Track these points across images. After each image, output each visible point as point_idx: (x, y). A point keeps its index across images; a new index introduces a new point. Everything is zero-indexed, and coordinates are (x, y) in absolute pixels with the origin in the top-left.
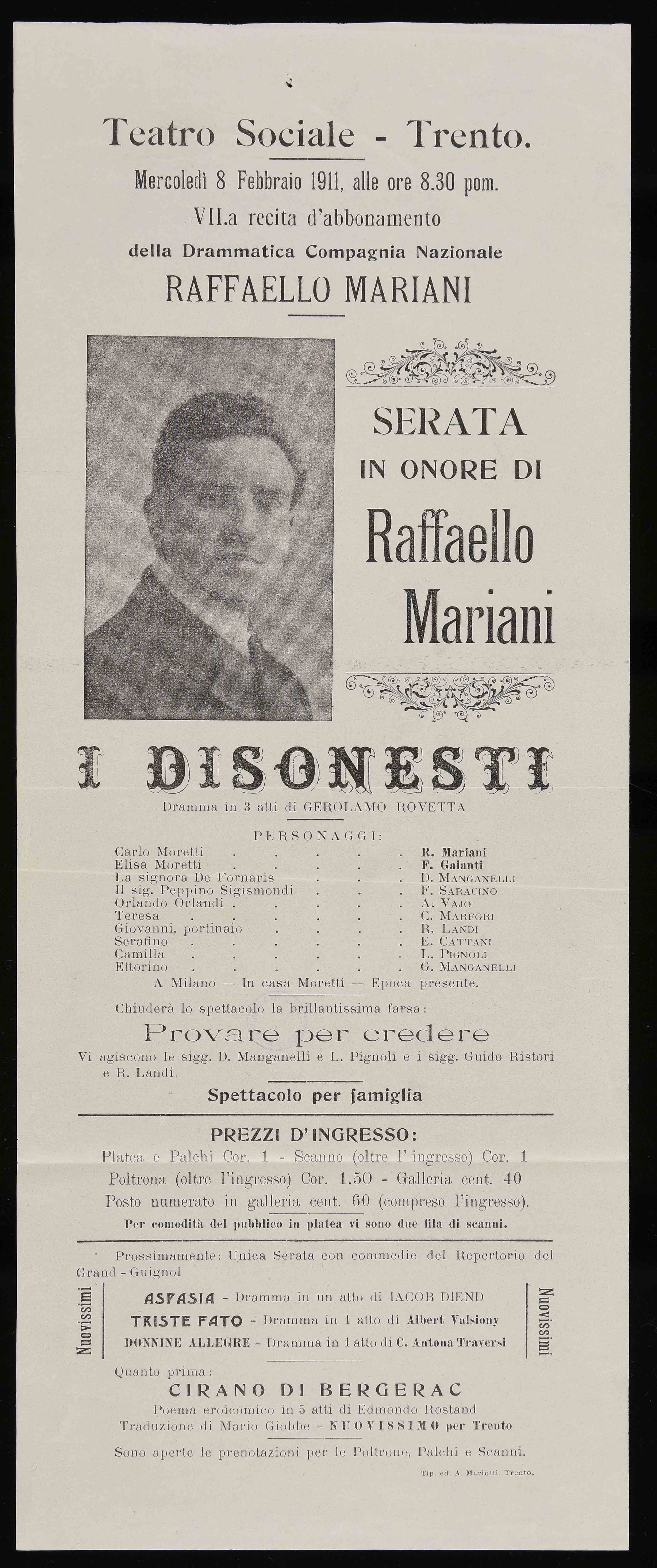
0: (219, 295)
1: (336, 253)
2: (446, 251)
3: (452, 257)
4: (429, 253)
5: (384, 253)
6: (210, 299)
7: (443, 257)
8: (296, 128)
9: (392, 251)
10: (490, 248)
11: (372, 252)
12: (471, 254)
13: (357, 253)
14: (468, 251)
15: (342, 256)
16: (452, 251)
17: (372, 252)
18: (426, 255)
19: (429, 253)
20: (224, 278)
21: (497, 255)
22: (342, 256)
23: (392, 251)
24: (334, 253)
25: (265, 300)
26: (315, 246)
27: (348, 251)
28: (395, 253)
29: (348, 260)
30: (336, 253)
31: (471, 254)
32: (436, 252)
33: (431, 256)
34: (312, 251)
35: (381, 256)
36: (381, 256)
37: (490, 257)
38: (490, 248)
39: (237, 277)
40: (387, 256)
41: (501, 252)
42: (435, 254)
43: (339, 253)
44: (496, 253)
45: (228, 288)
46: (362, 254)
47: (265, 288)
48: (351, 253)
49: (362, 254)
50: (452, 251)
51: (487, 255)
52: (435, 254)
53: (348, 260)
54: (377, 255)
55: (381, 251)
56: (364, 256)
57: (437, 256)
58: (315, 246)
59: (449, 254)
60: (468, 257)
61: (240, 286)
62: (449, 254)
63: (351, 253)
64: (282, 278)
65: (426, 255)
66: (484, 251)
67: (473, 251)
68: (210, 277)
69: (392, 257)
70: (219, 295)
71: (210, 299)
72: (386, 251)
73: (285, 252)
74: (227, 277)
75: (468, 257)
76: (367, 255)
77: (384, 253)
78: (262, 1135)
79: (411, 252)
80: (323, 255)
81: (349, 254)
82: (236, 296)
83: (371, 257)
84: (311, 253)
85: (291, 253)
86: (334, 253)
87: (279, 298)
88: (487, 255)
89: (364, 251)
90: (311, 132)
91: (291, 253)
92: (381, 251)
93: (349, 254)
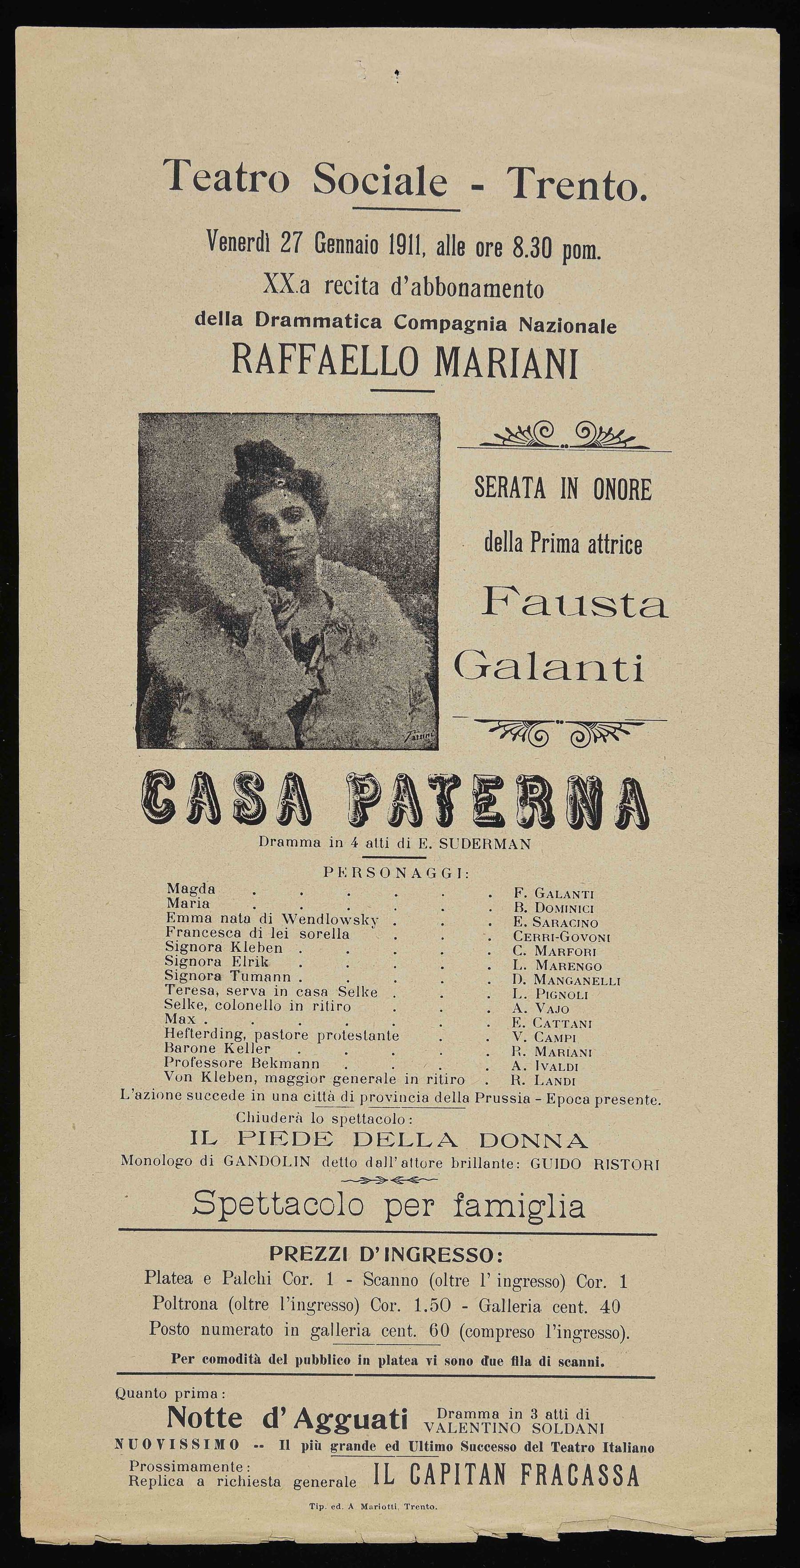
0: (293, 366)
1: (428, 323)
2: (553, 324)
3: (560, 331)
4: (533, 326)
5: (482, 325)
6: (283, 371)
7: (549, 330)
8: (382, 173)
9: (492, 323)
10: (603, 321)
11: (469, 323)
12: (581, 327)
13: (452, 324)
14: (578, 325)
15: (435, 328)
16: (560, 324)
17: (469, 323)
18: (530, 329)
19: (533, 326)
20: (298, 347)
21: (611, 329)
22: (435, 328)
23: (492, 323)
24: (426, 324)
25: (344, 372)
26: (405, 316)
27: (442, 321)
28: (495, 325)
29: (442, 332)
30: (428, 323)
31: (581, 327)
32: (542, 323)
33: (536, 329)
34: (402, 322)
35: (479, 329)
36: (479, 329)
37: (603, 332)
38: (603, 321)
39: (313, 345)
40: (486, 329)
41: (615, 326)
42: (539, 327)
43: (432, 324)
44: (609, 327)
45: (303, 358)
46: (457, 325)
47: (345, 359)
48: (445, 325)
49: (457, 325)
50: (560, 324)
51: (600, 329)
52: (539, 327)
53: (442, 332)
54: (475, 327)
55: (479, 322)
56: (460, 328)
57: (542, 330)
58: (405, 316)
59: (556, 327)
60: (577, 331)
61: (317, 356)
62: (556, 327)
63: (445, 325)
64: (365, 348)
65: (530, 329)
66: (596, 325)
67: (584, 325)
68: (283, 346)
69: (492, 329)
70: (293, 366)
71: (283, 371)
72: (485, 322)
73: (370, 322)
74: (302, 346)
75: (577, 331)
76: (464, 327)
77: (482, 325)
78: (327, 1254)
79: (513, 323)
80: (413, 326)
81: (442, 325)
82: (312, 367)
83: (467, 329)
84: (401, 324)
85: (377, 323)
86: (426, 324)
87: (360, 371)
88: (600, 329)
89: (460, 322)
90: (398, 179)
91: (377, 323)
92: (479, 322)
93: (442, 325)
